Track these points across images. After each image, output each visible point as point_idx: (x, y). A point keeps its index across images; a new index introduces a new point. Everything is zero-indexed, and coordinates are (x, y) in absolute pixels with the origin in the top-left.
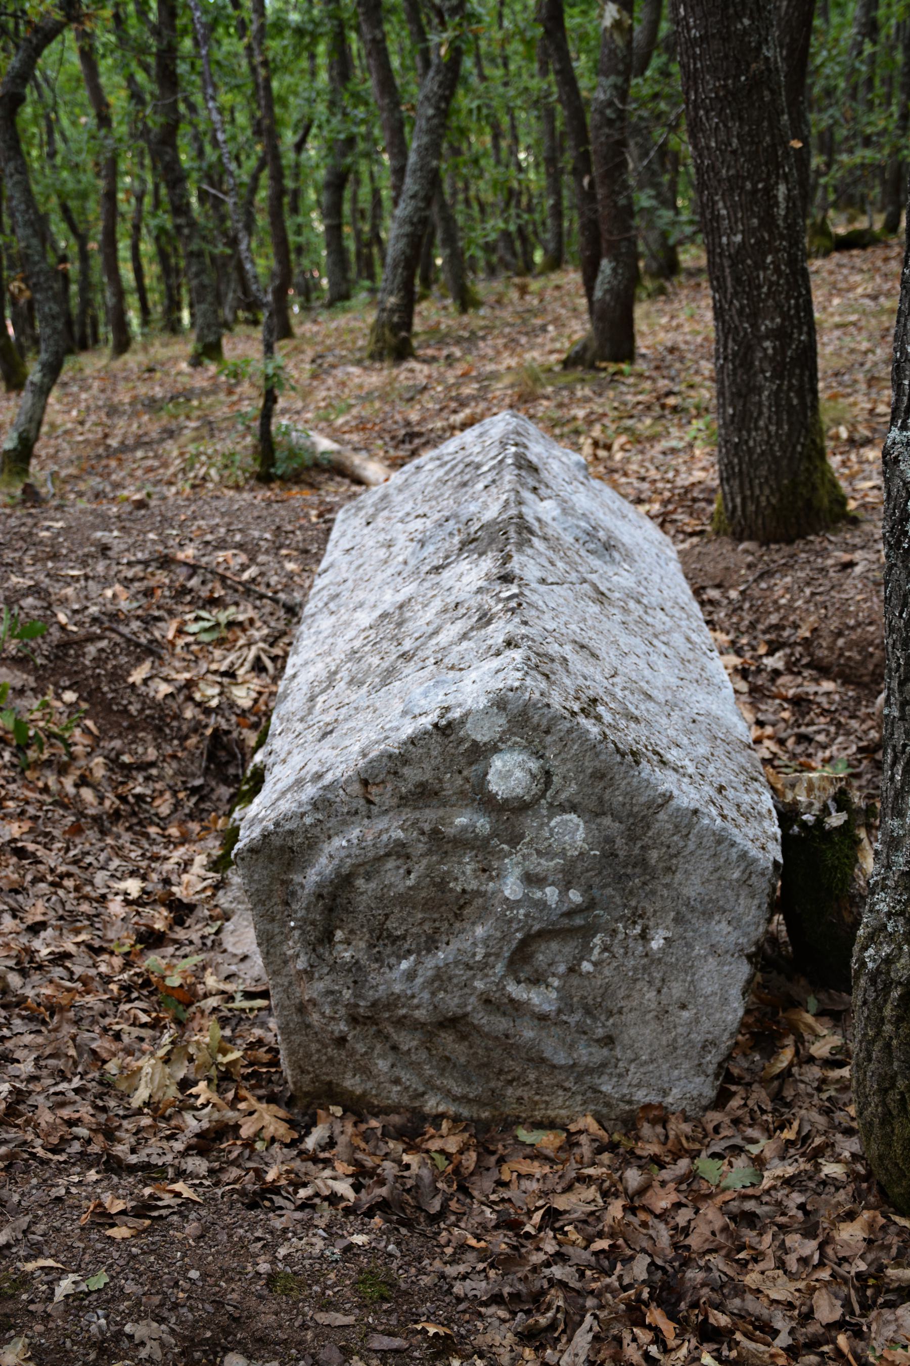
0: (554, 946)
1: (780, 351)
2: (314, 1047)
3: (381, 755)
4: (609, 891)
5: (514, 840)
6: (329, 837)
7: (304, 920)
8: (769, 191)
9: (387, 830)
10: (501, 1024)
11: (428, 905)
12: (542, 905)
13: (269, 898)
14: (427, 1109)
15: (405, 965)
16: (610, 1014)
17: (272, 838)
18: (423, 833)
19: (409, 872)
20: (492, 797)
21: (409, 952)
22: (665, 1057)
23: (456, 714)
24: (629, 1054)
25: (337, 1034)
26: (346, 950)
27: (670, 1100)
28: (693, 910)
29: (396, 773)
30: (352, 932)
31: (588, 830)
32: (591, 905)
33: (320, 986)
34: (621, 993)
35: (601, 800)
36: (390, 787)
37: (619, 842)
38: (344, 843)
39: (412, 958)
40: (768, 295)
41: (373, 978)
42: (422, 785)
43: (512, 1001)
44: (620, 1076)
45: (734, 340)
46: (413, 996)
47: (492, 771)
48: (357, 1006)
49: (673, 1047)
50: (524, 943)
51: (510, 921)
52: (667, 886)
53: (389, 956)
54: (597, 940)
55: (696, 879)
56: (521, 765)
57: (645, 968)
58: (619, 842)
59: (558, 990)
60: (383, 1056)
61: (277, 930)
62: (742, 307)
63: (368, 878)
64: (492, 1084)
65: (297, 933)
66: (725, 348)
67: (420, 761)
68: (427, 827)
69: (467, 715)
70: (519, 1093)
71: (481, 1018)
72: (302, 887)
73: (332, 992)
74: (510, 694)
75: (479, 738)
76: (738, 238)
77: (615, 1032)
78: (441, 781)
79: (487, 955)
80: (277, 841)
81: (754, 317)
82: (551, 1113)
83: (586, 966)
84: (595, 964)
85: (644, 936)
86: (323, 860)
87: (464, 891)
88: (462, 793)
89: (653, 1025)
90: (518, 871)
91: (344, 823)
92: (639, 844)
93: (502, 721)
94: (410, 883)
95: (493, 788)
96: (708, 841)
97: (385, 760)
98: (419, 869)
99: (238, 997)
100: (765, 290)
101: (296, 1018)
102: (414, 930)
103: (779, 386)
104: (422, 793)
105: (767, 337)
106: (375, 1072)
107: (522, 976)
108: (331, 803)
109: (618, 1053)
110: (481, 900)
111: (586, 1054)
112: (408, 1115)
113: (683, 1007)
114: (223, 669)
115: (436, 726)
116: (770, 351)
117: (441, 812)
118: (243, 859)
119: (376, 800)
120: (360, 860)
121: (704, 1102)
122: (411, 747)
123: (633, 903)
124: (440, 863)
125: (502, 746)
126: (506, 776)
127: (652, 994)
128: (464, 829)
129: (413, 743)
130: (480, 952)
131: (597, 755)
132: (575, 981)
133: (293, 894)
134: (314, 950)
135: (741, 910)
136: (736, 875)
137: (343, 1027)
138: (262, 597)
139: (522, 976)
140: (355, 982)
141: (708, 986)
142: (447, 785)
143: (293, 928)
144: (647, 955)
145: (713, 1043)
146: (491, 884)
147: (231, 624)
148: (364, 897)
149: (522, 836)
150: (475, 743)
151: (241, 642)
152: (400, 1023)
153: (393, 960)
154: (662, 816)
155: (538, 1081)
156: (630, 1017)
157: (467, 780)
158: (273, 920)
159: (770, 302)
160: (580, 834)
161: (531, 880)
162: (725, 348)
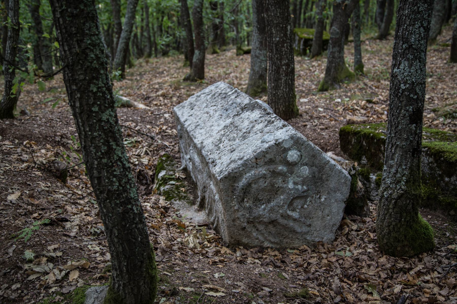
0: (298, 201)
1: (287, 69)
2: (236, 231)
3: (261, 151)
4: (313, 186)
5: (292, 173)
7: (238, 196)
8: (286, 27)
9: (261, 171)
10: (285, 222)
11: (269, 191)
12: (298, 190)
13: (228, 190)
14: (264, 246)
15: (263, 207)
16: (310, 218)
18: (270, 172)
20: (288, 162)
21: (263, 204)
22: (323, 229)
23: (281, 141)
24: (314, 229)
25: (243, 226)
27: (324, 240)
28: (332, 190)
30: (249, 199)
31: (309, 170)
32: (308, 190)
33: (241, 213)
34: (313, 213)
35: (313, 163)
36: (262, 160)
37: (317, 173)
40: (285, 54)
41: (254, 211)
42: (271, 159)
43: (288, 215)
44: (312, 235)
45: (275, 66)
48: (250, 218)
49: (325, 226)
50: (292, 200)
51: (290, 194)
52: (326, 184)
54: (308, 199)
55: (333, 183)
56: (296, 153)
57: (320, 206)
58: (317, 173)
59: (299, 212)
60: (255, 232)
62: (278, 57)
63: (255, 183)
64: (280, 239)
65: (235, 199)
66: (272, 68)
67: (271, 153)
68: (271, 170)
69: (283, 140)
70: (286, 241)
71: (281, 221)
72: (238, 187)
73: (244, 215)
75: (286, 147)
76: (278, 39)
77: (311, 223)
78: (275, 158)
79: (283, 203)
80: (232, 175)
81: (281, 60)
82: (294, 246)
83: (306, 206)
84: (308, 206)
85: (320, 198)
86: (244, 180)
87: (278, 187)
88: (280, 161)
89: (321, 221)
90: (292, 181)
91: (250, 170)
92: (321, 174)
93: (292, 142)
94: (265, 185)
95: (289, 159)
96: (337, 173)
97: (262, 153)
98: (268, 181)
99: (197, 226)
100: (284, 53)
101: (232, 223)
103: (287, 78)
105: (284, 65)
106: (252, 236)
107: (290, 209)
108: (247, 164)
109: (312, 229)
110: (282, 189)
111: (305, 229)
113: (328, 216)
114: (136, 154)
115: (275, 144)
116: (284, 69)
117: (275, 166)
119: (259, 163)
120: (254, 179)
121: (332, 240)
125: (291, 149)
126: (292, 156)
127: (320, 213)
128: (281, 170)
130: (282, 202)
131: (313, 151)
132: (303, 210)
133: (235, 189)
135: (343, 190)
136: (343, 181)
137: (245, 224)
138: (143, 134)
139: (290, 209)
141: (334, 210)
142: (277, 159)
145: (335, 225)
147: (136, 142)
149: (294, 172)
150: (285, 148)
151: (140, 147)
152: (260, 222)
153: (260, 206)
154: (327, 166)
155: (292, 237)
156: (315, 219)
157: (282, 157)
158: (229, 196)
159: (285, 56)
160: (307, 172)
161: (295, 183)
162: (272, 68)
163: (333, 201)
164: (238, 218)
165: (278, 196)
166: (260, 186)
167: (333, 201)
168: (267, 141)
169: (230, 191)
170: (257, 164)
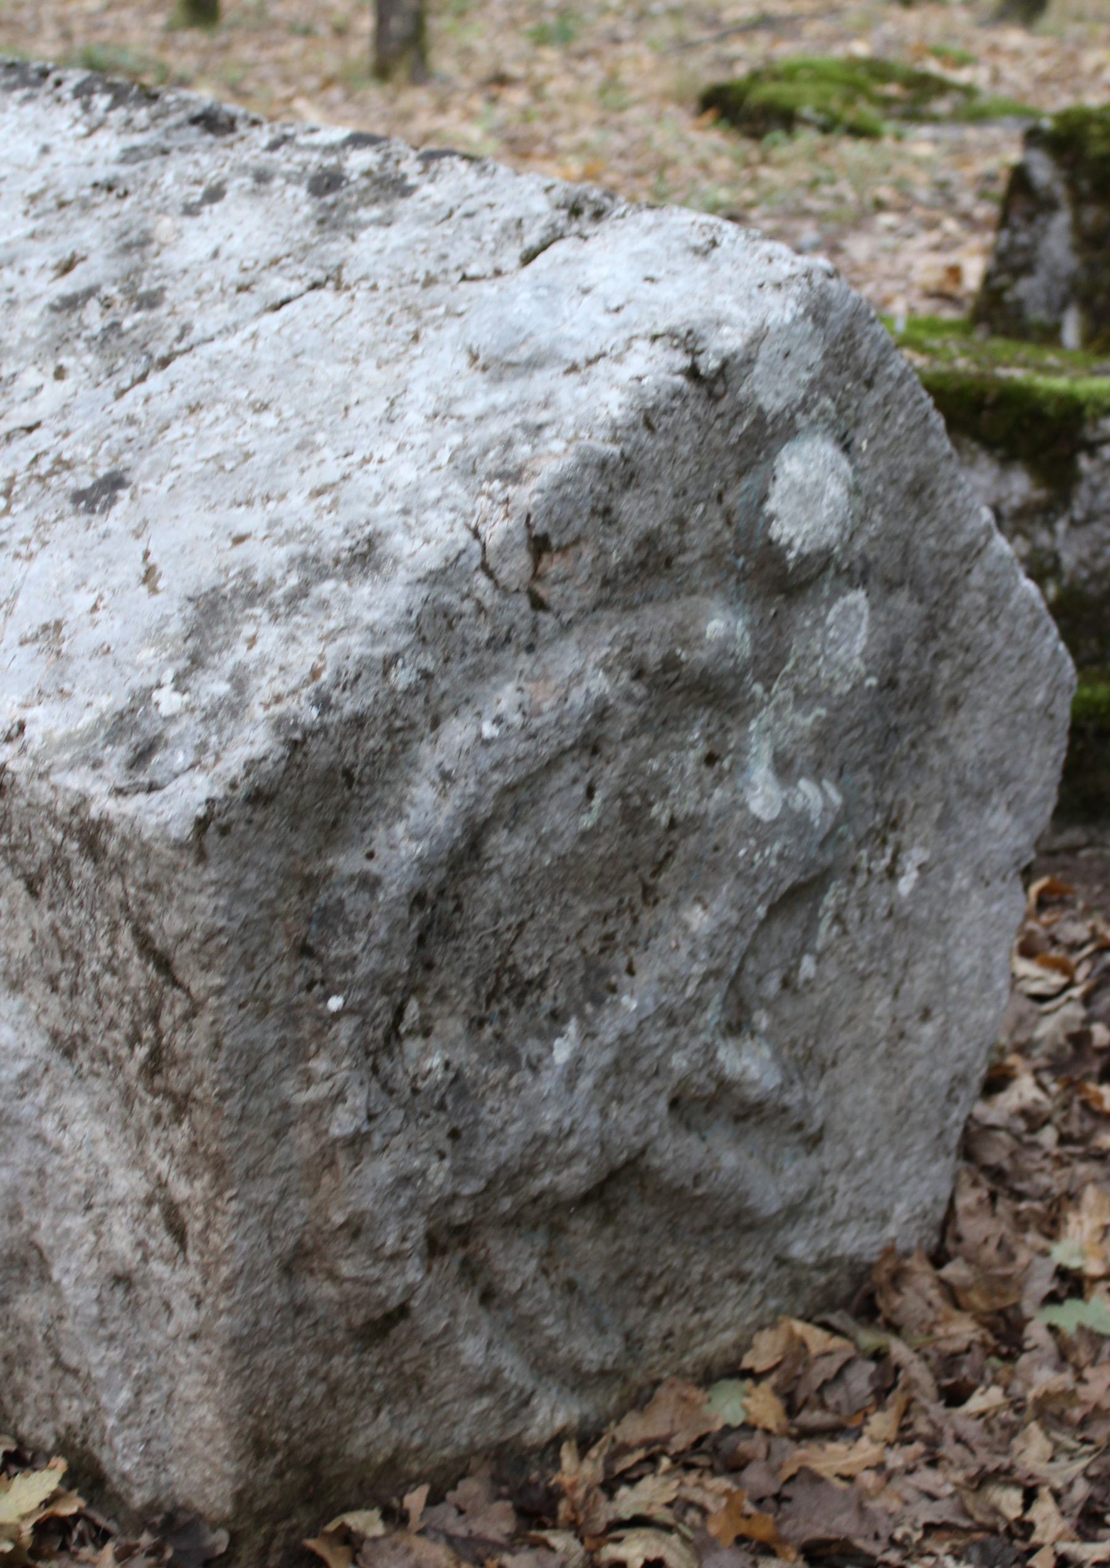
6: (435, 723)
9: (578, 677)
15: (562, 1052)
17: (313, 746)
19: (590, 792)
20: (773, 552)
21: (557, 1017)
24: (841, 1155)
26: (426, 1052)
29: (607, 511)
31: (874, 623)
36: (588, 553)
37: (910, 647)
38: (489, 730)
39: (572, 1028)
42: (649, 540)
46: (571, 1132)
47: (778, 490)
49: (904, 1111)
53: (522, 1037)
57: (887, 940)
58: (910, 647)
61: (272, 1039)
65: (345, 1029)
69: (758, 339)
72: (369, 883)
74: (833, 283)
78: (681, 523)
80: (321, 755)
83: (808, 966)
85: (892, 874)
86: (424, 793)
87: (673, 824)
91: (477, 674)
92: (934, 647)
94: (587, 821)
95: (780, 531)
102: (570, 953)
104: (643, 565)
108: (448, 618)
112: (485, 1472)
113: (926, 1015)
117: (676, 610)
118: (224, 831)
119: (549, 592)
122: (644, 436)
123: (888, 797)
124: (650, 754)
125: (802, 421)
126: (808, 496)
127: (883, 1006)
129: (649, 425)
134: (375, 1069)
137: (413, 1273)
140: (454, 1134)
143: (337, 1016)
144: (890, 914)
146: (718, 793)
148: (494, 884)
153: (532, 1047)
154: (977, 578)
163: (962, 880)
164: (355, 1228)
165: (663, 912)
166: (543, 842)
167: (962, 880)
168: (578, 355)
169: (280, 945)
170: (538, 604)
